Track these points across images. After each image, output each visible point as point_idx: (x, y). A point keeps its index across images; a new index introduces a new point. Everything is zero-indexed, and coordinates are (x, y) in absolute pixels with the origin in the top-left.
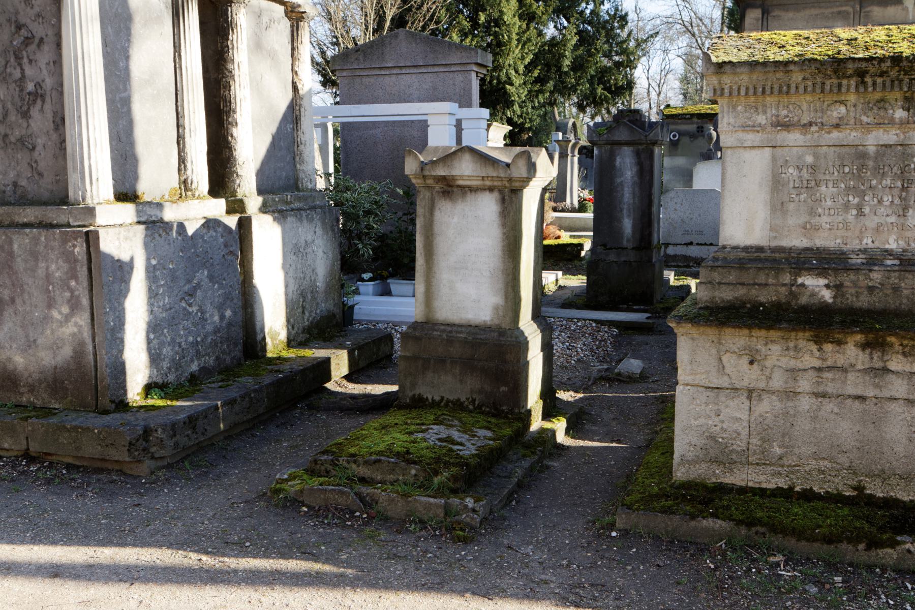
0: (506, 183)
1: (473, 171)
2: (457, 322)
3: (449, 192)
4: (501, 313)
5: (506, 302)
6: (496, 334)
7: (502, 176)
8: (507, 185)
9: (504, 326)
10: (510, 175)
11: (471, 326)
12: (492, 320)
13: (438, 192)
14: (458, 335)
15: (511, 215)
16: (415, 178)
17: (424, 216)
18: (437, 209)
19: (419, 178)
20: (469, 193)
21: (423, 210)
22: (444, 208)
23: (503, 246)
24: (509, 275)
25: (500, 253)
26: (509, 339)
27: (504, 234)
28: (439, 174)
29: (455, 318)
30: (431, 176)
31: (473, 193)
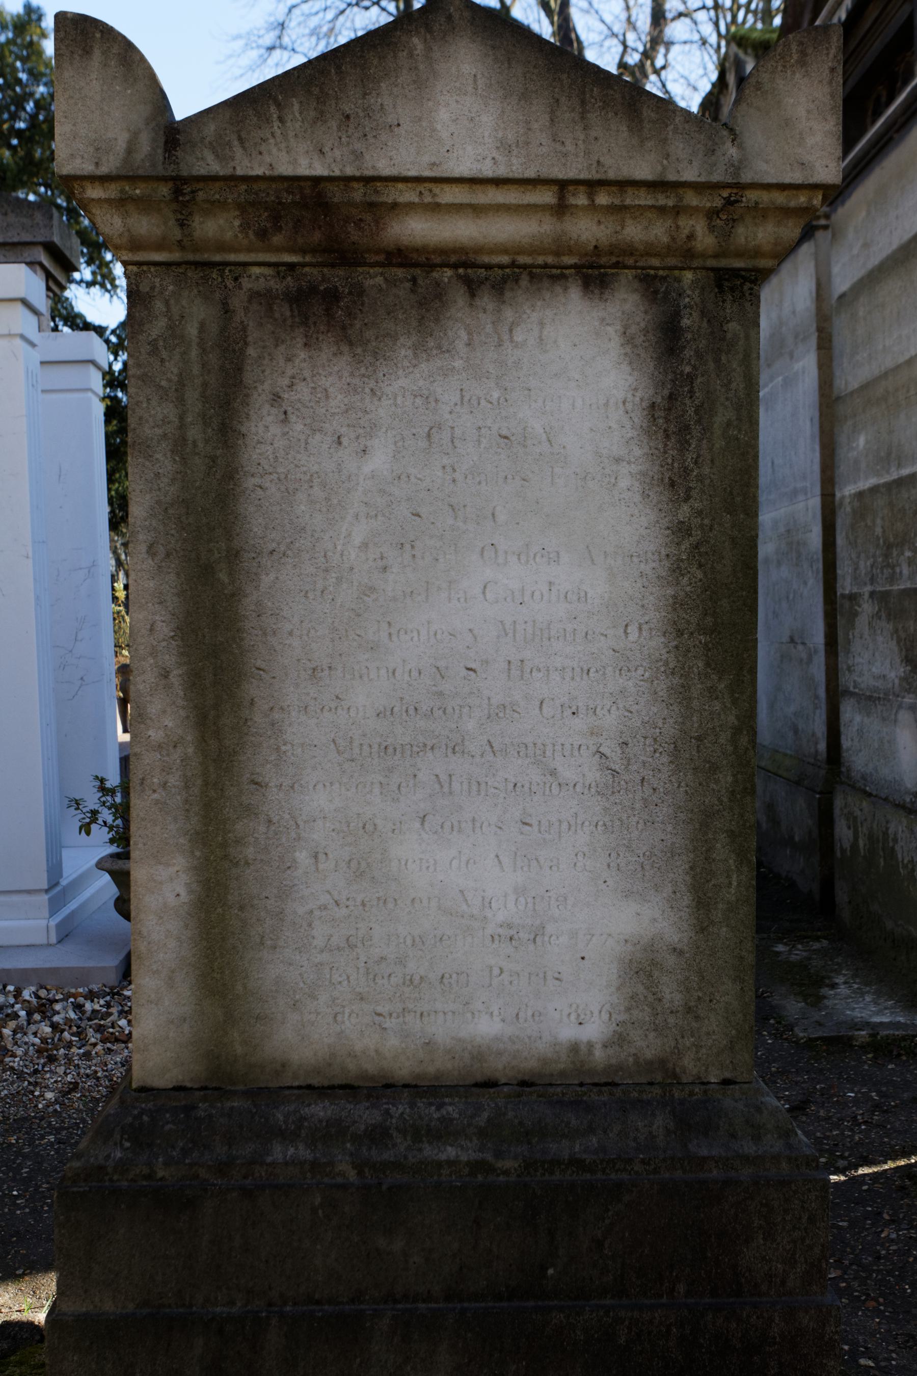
0: (699, 226)
1: (505, 147)
2: (404, 1069)
3: (332, 297)
4: (672, 995)
5: (702, 928)
6: (660, 1122)
7: (690, 175)
8: (705, 240)
9: (689, 1064)
10: (737, 167)
11: (490, 1084)
12: (619, 1039)
13: (265, 298)
14: (429, 1151)
15: (719, 419)
16: (121, 203)
17: (180, 446)
18: (260, 398)
19: (145, 205)
20: (459, 297)
21: (169, 410)
22: (303, 391)
23: (677, 604)
24: (714, 768)
25: (656, 644)
26: (749, 1148)
27: (681, 530)
28: (285, 169)
29: (393, 1042)
30: (233, 179)
31: (486, 300)
